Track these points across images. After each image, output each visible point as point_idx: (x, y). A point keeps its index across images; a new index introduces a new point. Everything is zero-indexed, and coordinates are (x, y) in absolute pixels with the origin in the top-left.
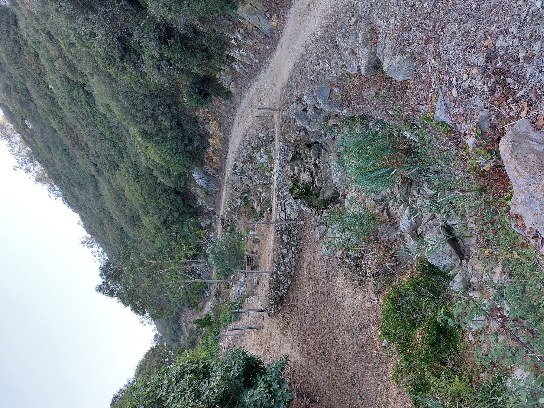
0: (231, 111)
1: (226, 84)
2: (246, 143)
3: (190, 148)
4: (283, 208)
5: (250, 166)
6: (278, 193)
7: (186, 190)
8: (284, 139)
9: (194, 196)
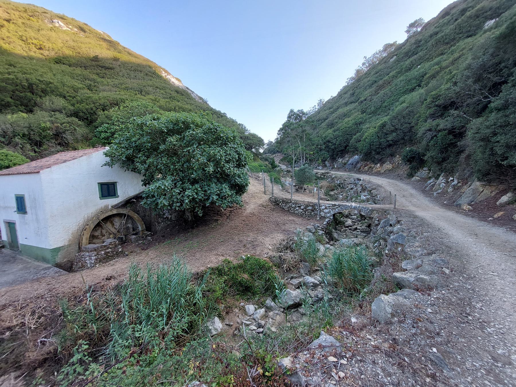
0: (400, 178)
1: (419, 174)
2: (374, 186)
3: (374, 153)
5: (359, 189)
7: (347, 152)
8: (374, 210)
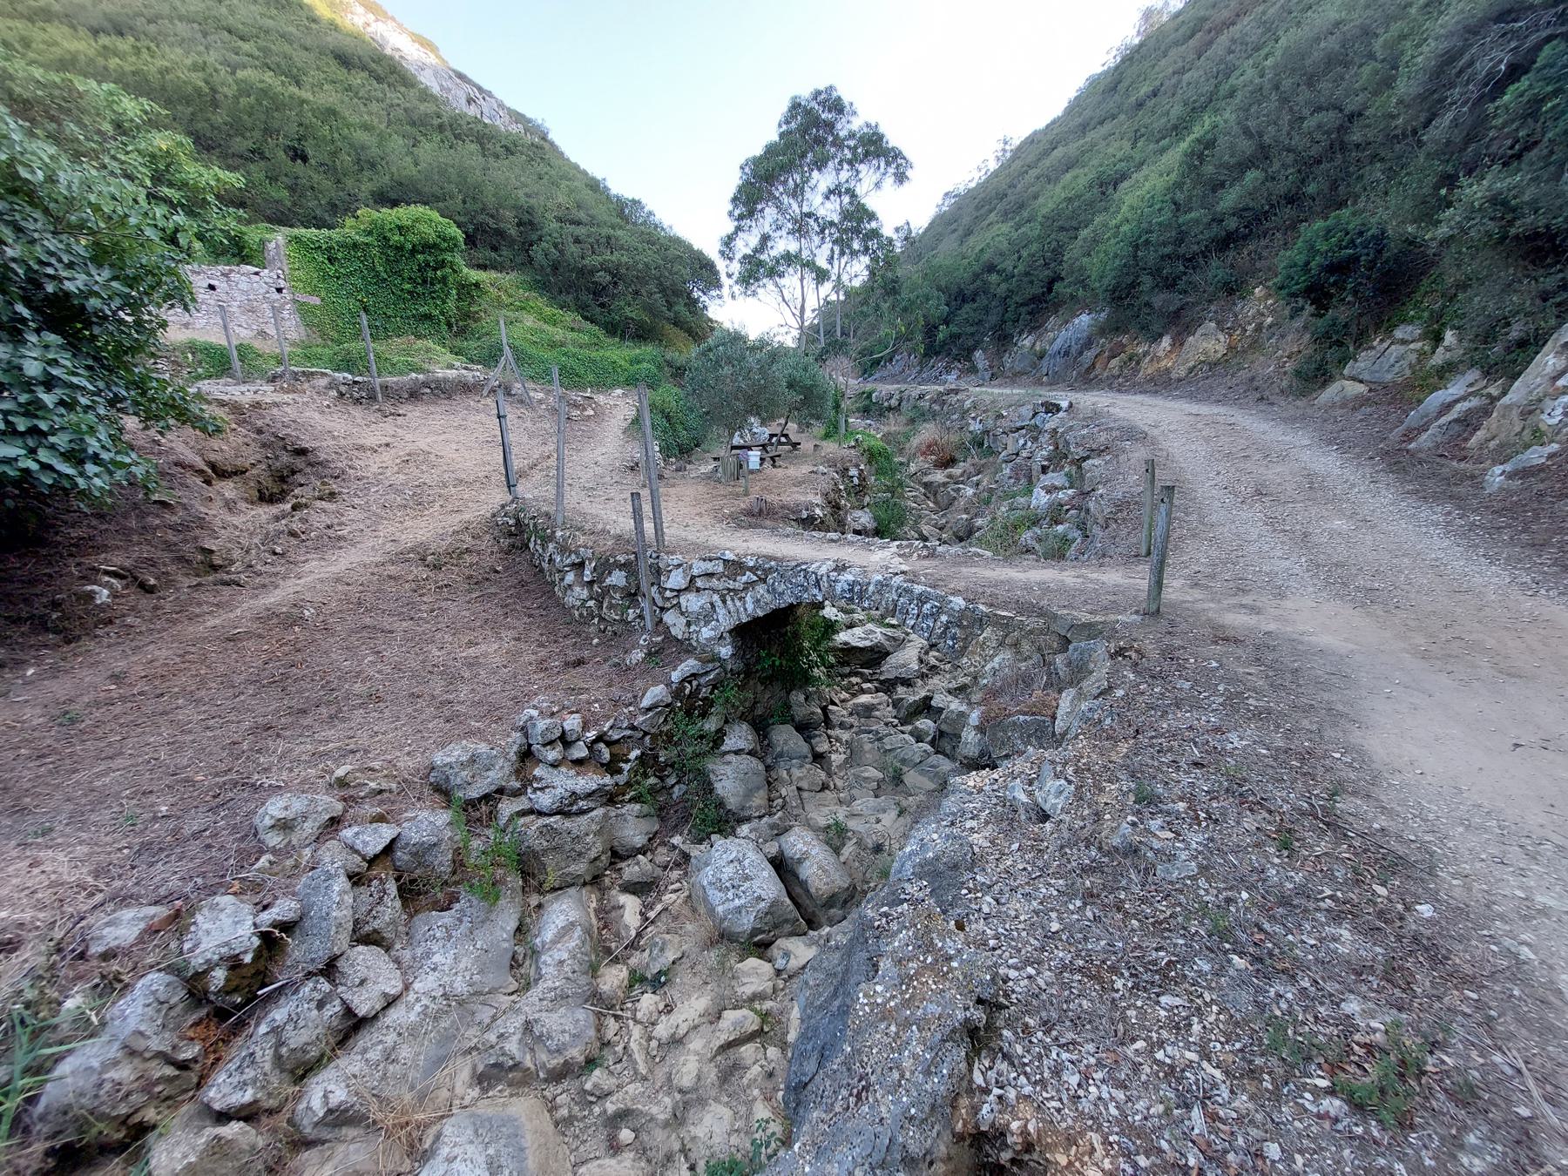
0: (1258, 395)
1: (1363, 363)
2: (1103, 438)
3: (1147, 281)
4: (699, 583)
5: (1042, 454)
6: (751, 569)
7: (1056, 307)
8: (980, 621)
9: (1039, 327)
